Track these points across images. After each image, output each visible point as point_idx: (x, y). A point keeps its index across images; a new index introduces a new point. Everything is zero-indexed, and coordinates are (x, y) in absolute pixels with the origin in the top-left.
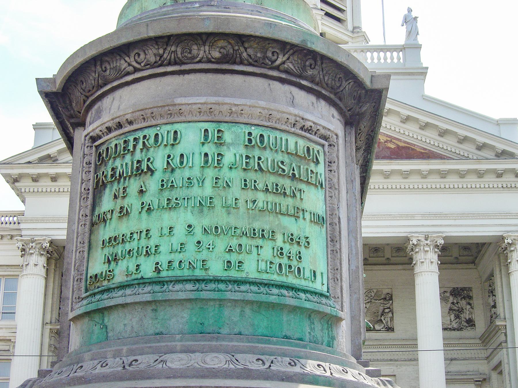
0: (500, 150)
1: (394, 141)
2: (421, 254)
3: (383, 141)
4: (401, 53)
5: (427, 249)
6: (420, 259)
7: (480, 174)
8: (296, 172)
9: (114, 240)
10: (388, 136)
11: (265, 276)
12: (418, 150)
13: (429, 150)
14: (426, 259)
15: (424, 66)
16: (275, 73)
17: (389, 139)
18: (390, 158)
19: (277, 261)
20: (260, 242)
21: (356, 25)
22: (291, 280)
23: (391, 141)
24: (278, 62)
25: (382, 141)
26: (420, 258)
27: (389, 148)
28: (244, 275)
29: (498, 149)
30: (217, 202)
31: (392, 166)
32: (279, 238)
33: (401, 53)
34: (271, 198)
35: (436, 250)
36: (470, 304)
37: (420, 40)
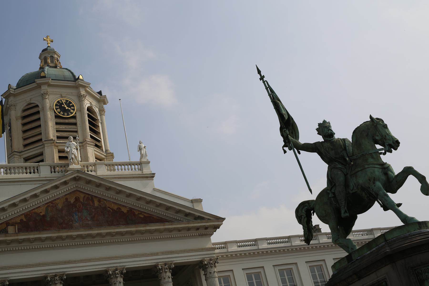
0: (197, 216)
1: (143, 213)
2: (163, 274)
3: (137, 214)
5: (166, 270)
6: (163, 277)
7: (189, 229)
10: (139, 211)
13: (161, 218)
14: (166, 276)
17: (139, 212)
18: (141, 223)
23: (141, 214)
25: (136, 214)
26: (163, 276)
27: (141, 217)
29: (196, 215)
31: (146, 228)
35: (171, 271)
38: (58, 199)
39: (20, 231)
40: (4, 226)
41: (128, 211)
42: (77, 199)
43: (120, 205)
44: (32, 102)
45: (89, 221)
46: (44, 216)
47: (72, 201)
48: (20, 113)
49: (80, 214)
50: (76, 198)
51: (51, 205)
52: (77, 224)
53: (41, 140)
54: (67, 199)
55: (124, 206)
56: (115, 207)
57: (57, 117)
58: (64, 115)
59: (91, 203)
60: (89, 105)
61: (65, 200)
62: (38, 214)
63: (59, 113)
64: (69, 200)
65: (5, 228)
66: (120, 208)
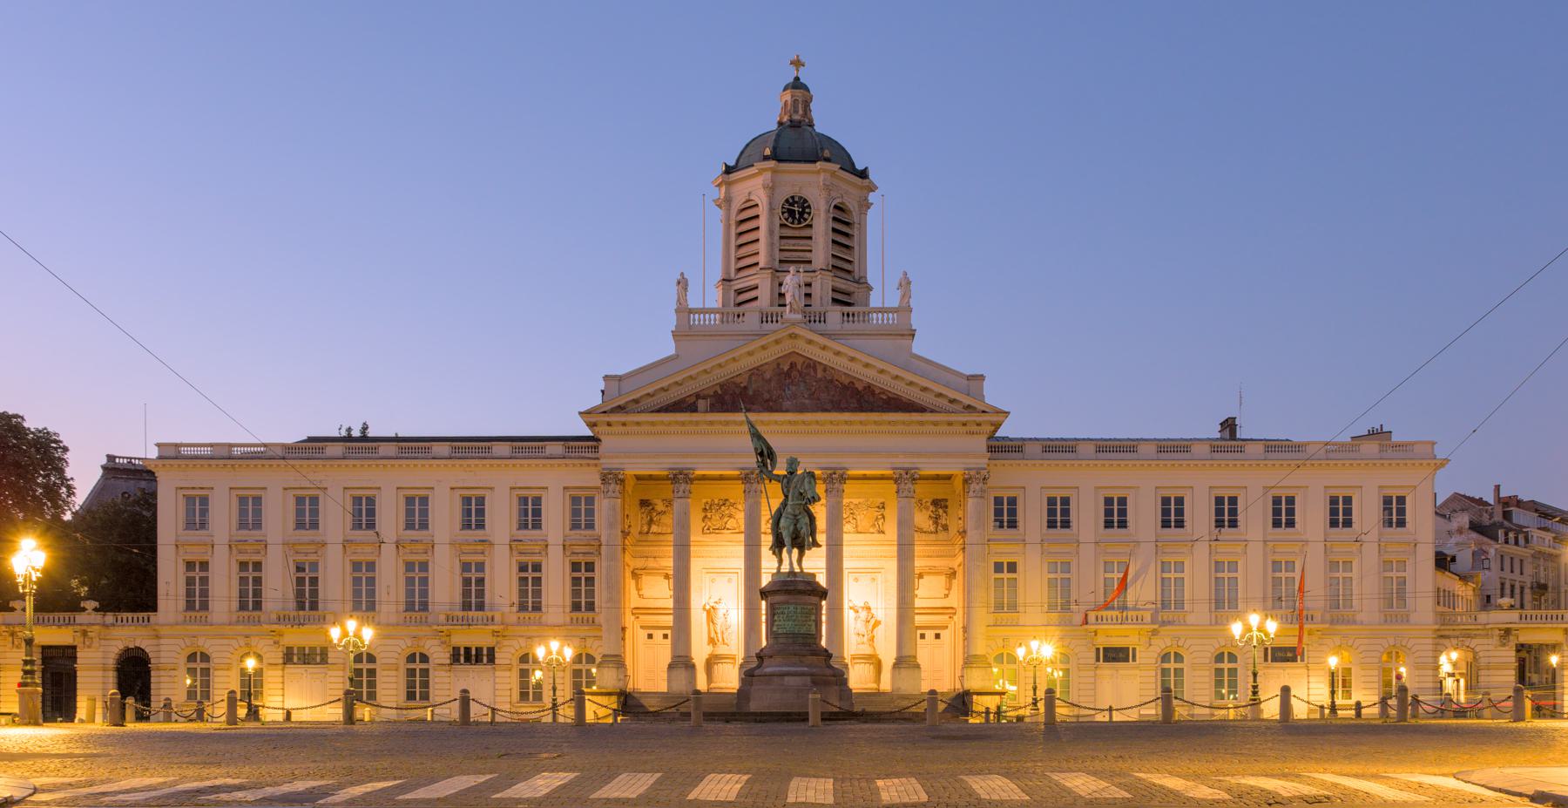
4: (895, 315)
9: (777, 625)
10: (882, 389)
12: (904, 400)
15: (913, 328)
21: (862, 275)
23: (884, 393)
27: (883, 399)
33: (895, 315)
36: (945, 512)
37: (913, 303)
38: (766, 364)
39: (713, 409)
40: (693, 399)
41: (865, 388)
42: (793, 365)
43: (855, 378)
44: (752, 198)
45: (806, 399)
46: (745, 388)
47: (786, 368)
48: (734, 218)
49: (794, 388)
50: (791, 364)
51: (756, 372)
52: (790, 403)
53: (757, 264)
54: (778, 365)
55: (859, 380)
56: (846, 382)
57: (782, 226)
58: (793, 223)
59: (812, 373)
60: (839, 200)
61: (775, 367)
62: (737, 385)
63: (787, 220)
64: (781, 367)
65: (694, 403)
66: (853, 383)
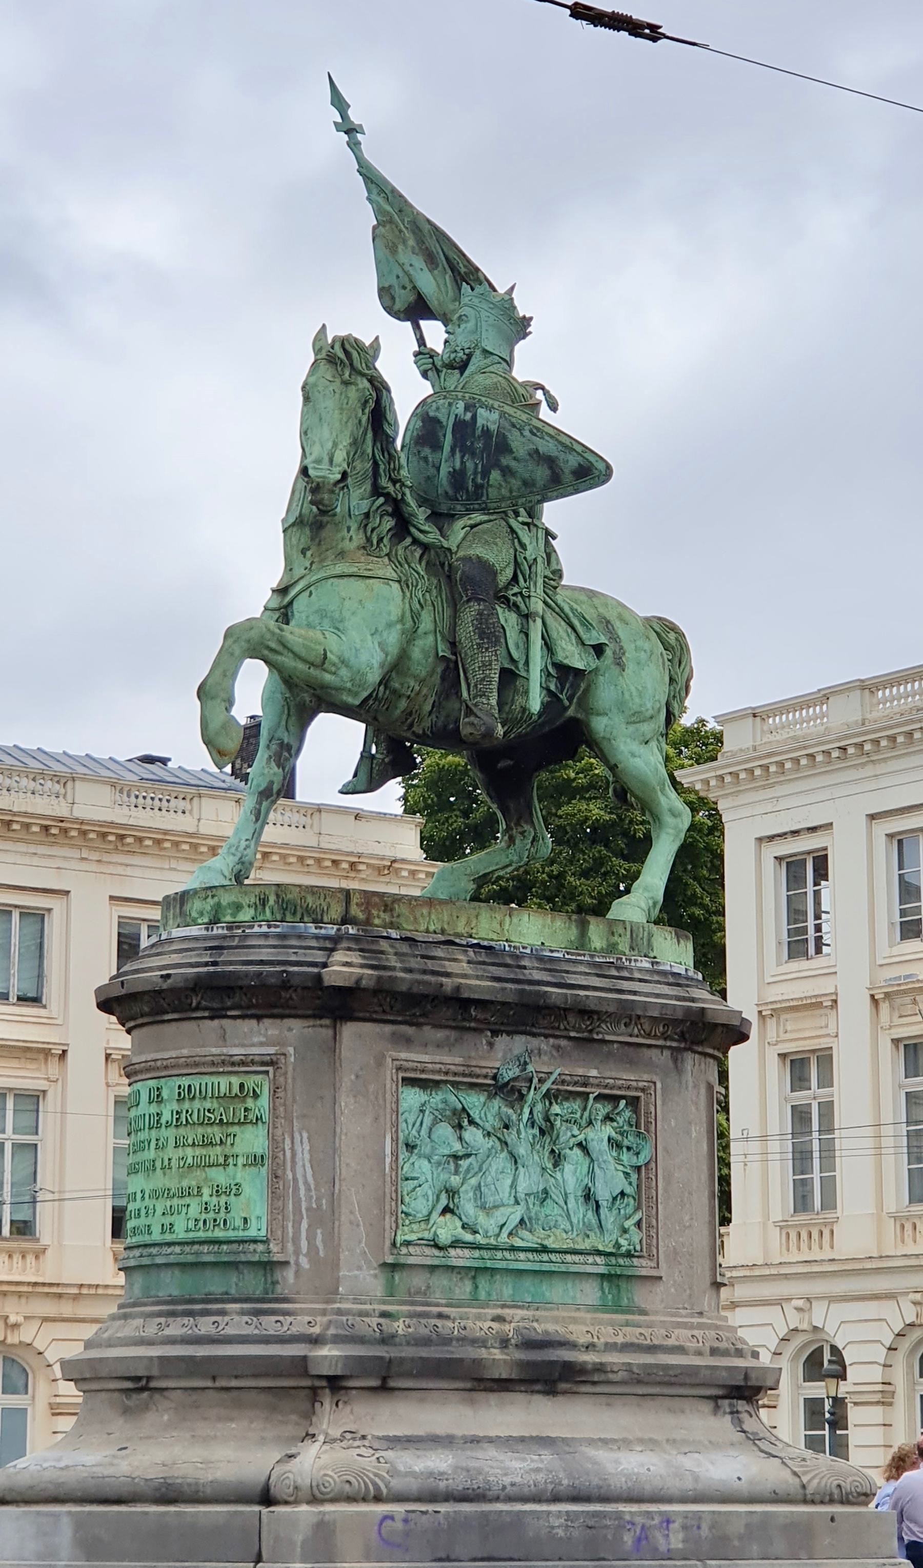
8: (224, 1117)
11: (191, 1235)
16: (199, 1014)
19: (204, 1216)
20: (187, 1200)
22: (219, 1234)
24: (194, 1004)
28: (174, 1236)
30: (158, 1164)
32: (206, 1191)
34: (198, 1151)
